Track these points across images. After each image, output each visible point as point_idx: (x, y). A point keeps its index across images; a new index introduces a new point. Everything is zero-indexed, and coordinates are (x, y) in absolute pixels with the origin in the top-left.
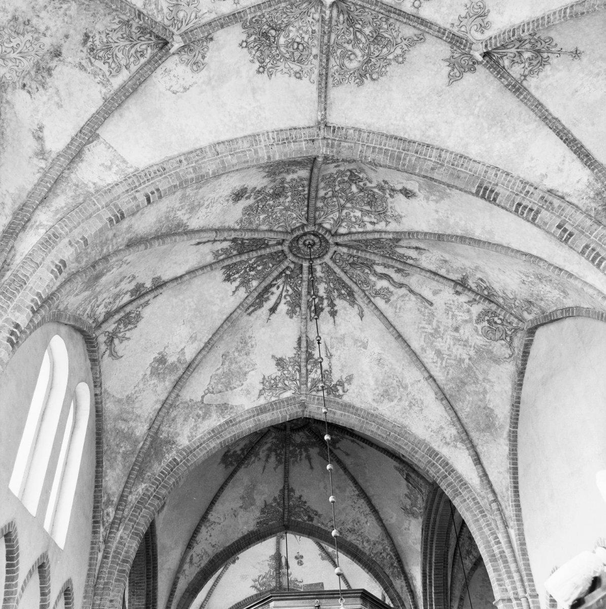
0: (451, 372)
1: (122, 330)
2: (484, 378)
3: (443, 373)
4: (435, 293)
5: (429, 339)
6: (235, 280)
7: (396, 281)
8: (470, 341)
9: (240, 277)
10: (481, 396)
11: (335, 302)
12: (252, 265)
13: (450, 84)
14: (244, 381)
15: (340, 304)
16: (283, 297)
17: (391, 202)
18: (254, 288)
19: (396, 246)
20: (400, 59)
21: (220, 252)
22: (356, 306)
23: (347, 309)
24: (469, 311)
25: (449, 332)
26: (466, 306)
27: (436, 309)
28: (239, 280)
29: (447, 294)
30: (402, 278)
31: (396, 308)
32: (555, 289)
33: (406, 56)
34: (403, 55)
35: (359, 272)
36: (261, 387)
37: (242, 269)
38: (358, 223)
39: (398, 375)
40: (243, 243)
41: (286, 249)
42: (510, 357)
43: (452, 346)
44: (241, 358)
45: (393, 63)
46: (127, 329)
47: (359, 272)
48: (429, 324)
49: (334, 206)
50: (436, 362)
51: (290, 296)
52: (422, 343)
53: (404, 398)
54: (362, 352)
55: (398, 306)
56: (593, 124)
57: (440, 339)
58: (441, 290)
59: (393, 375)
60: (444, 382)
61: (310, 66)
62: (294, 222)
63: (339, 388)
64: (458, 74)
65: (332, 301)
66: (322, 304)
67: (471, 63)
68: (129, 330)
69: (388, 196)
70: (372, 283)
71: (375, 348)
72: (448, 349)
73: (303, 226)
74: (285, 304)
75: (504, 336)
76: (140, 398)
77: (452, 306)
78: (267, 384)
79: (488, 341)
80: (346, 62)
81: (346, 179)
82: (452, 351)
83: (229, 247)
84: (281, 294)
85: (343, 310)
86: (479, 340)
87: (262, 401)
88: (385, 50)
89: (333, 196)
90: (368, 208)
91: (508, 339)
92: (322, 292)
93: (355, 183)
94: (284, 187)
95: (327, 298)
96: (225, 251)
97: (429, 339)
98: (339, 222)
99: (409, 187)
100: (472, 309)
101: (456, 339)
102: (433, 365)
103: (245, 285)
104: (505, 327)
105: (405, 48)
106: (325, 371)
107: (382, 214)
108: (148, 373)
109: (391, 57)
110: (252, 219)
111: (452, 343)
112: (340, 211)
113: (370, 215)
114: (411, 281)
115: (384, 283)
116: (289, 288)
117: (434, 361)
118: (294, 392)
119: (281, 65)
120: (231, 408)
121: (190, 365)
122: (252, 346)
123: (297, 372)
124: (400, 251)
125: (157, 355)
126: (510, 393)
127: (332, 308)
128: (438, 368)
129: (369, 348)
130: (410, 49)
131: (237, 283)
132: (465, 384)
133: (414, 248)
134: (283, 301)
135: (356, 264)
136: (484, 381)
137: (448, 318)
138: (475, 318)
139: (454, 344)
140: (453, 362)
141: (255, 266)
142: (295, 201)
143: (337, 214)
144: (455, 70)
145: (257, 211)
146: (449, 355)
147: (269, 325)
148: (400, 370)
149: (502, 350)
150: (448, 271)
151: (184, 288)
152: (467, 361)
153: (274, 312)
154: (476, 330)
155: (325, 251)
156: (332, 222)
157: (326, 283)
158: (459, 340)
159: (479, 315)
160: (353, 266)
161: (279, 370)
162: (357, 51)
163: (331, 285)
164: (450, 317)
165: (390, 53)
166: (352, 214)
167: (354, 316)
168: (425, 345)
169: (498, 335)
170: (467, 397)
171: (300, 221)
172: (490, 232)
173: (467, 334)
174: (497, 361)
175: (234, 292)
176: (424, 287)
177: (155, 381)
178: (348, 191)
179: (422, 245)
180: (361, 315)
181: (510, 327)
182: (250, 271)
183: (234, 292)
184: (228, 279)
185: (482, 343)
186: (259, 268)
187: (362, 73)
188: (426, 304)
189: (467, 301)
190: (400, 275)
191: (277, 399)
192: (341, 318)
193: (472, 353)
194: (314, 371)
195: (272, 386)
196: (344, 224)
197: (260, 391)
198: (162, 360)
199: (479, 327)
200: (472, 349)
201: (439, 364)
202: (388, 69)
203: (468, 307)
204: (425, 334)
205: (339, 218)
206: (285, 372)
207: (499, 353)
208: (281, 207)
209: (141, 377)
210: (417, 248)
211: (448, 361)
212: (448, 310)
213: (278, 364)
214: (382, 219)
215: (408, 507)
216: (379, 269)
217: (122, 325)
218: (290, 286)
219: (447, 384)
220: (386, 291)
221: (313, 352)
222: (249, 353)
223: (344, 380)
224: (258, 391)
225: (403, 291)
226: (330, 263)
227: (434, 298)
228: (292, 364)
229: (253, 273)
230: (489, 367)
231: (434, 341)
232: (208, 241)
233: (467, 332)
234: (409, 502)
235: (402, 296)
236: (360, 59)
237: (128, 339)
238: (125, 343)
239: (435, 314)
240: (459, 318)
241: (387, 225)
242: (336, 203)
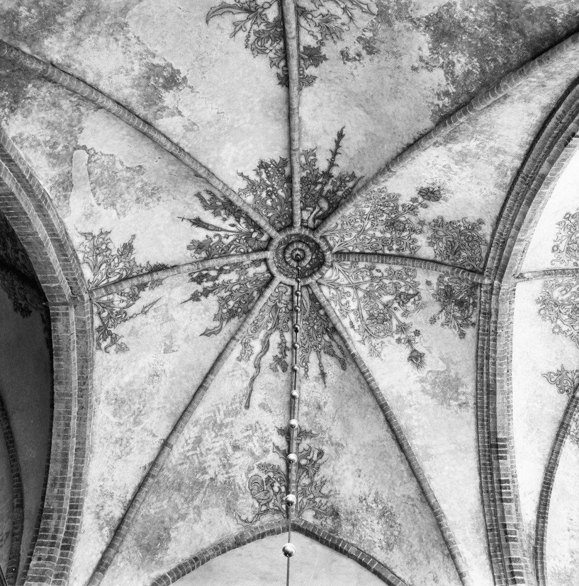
0: (185, 466)
1: (255, 27)
2: (198, 507)
3: (180, 459)
4: (263, 406)
5: (210, 423)
6: (259, 174)
7: (262, 359)
8: (233, 469)
9: (261, 180)
10: (176, 516)
11: (211, 295)
12: (275, 194)
13: (543, 375)
14: (104, 205)
15: (212, 303)
16: (218, 232)
17: (389, 342)
18: (244, 199)
19: (318, 353)
20: (557, 330)
21: (312, 158)
22: (217, 324)
23: (207, 313)
24: (266, 451)
25: (227, 441)
26: (269, 446)
27: (245, 414)
28: (258, 179)
29: (274, 421)
30: (268, 365)
31: (233, 371)
32: (384, 535)
33: (560, 335)
34: (560, 331)
35: (267, 317)
36: (96, 233)
37: (271, 182)
38: (343, 308)
39: (148, 405)
40: (316, 184)
41: (296, 230)
42: (245, 521)
43: (212, 452)
44: (133, 192)
45: (553, 325)
46: (252, 34)
47: (267, 317)
48: (225, 415)
49: (357, 278)
50: (188, 444)
51: (220, 240)
52: (203, 418)
53: (123, 428)
54: (160, 349)
55: (235, 373)
56: (558, 500)
57: (213, 434)
58: (271, 412)
59: (144, 401)
60: (170, 465)
61: (566, 259)
62: (337, 239)
63: (109, 340)
64: (553, 380)
65: (211, 291)
66: (207, 281)
67: (566, 388)
68: (248, 36)
69: (396, 336)
70: (256, 336)
71: (170, 363)
72: (208, 449)
73: (330, 249)
74: (207, 236)
75: (264, 502)
76: (113, 46)
77: (259, 431)
78: (101, 240)
79: (247, 488)
80: (561, 288)
81: (403, 290)
82: (207, 454)
83: (316, 168)
84: (222, 230)
85: (202, 307)
86: (241, 479)
87: (77, 240)
88: (566, 317)
89: (373, 278)
90: (366, 316)
91: (264, 508)
92: (223, 278)
93: (395, 299)
94: (404, 230)
95: (215, 285)
96: (310, 164)
97: (210, 423)
98: (334, 285)
99: (428, 359)
100: (271, 453)
101: (224, 453)
102: (183, 442)
103: (250, 187)
104: (274, 498)
105: (570, 333)
106: (125, 313)
107: (368, 334)
108: (156, 61)
109: (559, 322)
110: (371, 201)
111: (217, 450)
112: (349, 285)
113: (359, 319)
114: (266, 376)
115: (257, 346)
116: (231, 238)
117: (189, 441)
118: (91, 281)
119: (565, 233)
120: (65, 196)
121: (149, 124)
122: (146, 205)
123: (118, 276)
124: (313, 357)
125: (182, 76)
126: (205, 547)
127: (202, 294)
128: (182, 450)
129: (167, 355)
130: (568, 337)
131: (253, 177)
132: (179, 490)
133: (322, 371)
134: (211, 234)
135: (276, 312)
136: (194, 508)
137: (242, 432)
138: (263, 461)
139: (217, 453)
140: (197, 463)
141: (274, 197)
142: (374, 240)
143: (346, 282)
144: (556, 377)
145: (381, 205)
146: (201, 454)
147: (173, 220)
148: (156, 406)
149: (247, 508)
150: (307, 414)
151: (270, 113)
152: (207, 477)
153: (194, 224)
154: (250, 470)
155: (286, 273)
156: (334, 278)
157: (238, 280)
158: (226, 457)
159: (270, 465)
160: (274, 309)
161: (118, 250)
162: (568, 295)
163: (237, 287)
164: (245, 434)
165: (563, 321)
166: (350, 299)
167: (201, 325)
168: (201, 422)
169: (261, 495)
170: (165, 502)
171: (337, 245)
172: (429, 456)
173: (240, 462)
174: (230, 509)
175: (242, 175)
176: (263, 392)
177: (138, 69)
178: (382, 292)
179: (331, 379)
180: (207, 333)
181: (278, 504)
182: (268, 192)
183: (242, 175)
184: (263, 165)
185: (240, 483)
186: (269, 202)
187: (547, 302)
188: (245, 401)
189: (276, 445)
190: (271, 361)
191: (81, 260)
192: (192, 309)
193: (221, 478)
194: (123, 298)
195: (98, 249)
196: (333, 291)
197: (91, 234)
198: (173, 81)
199: (256, 471)
200: (226, 476)
201: (186, 448)
202: (548, 321)
203: (271, 449)
204: (213, 415)
205: (340, 285)
206: (116, 260)
207: (240, 507)
208: (369, 226)
209: (152, 49)
210: (323, 375)
211: (195, 457)
212: (252, 428)
213: (125, 246)
214: (362, 334)
216: (275, 338)
217: (264, 28)
218: (235, 240)
219: (169, 470)
220: (249, 353)
221: (147, 289)
222: (138, 203)
223: (119, 342)
224: (90, 231)
225: (252, 371)
226: (275, 283)
227: (257, 408)
228: (128, 265)
229: (264, 195)
230: (217, 505)
231: (208, 428)
232: (338, 145)
233: (241, 460)
235: (246, 372)
236: (560, 298)
237: (234, 34)
238: (231, 29)
239: (239, 416)
240: (250, 444)
241: (359, 342)
242: (361, 280)
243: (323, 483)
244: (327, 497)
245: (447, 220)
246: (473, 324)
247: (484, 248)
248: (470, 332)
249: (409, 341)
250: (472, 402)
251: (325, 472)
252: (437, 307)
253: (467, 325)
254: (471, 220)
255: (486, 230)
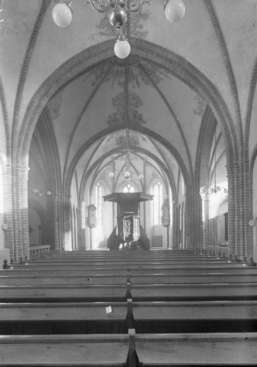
245: (138, 139)
246: (119, 146)
247: (134, 145)
248: (117, 146)
249: (111, 137)
250: (105, 153)
252: (119, 137)
253: (118, 145)
254: (140, 143)
255: (138, 146)
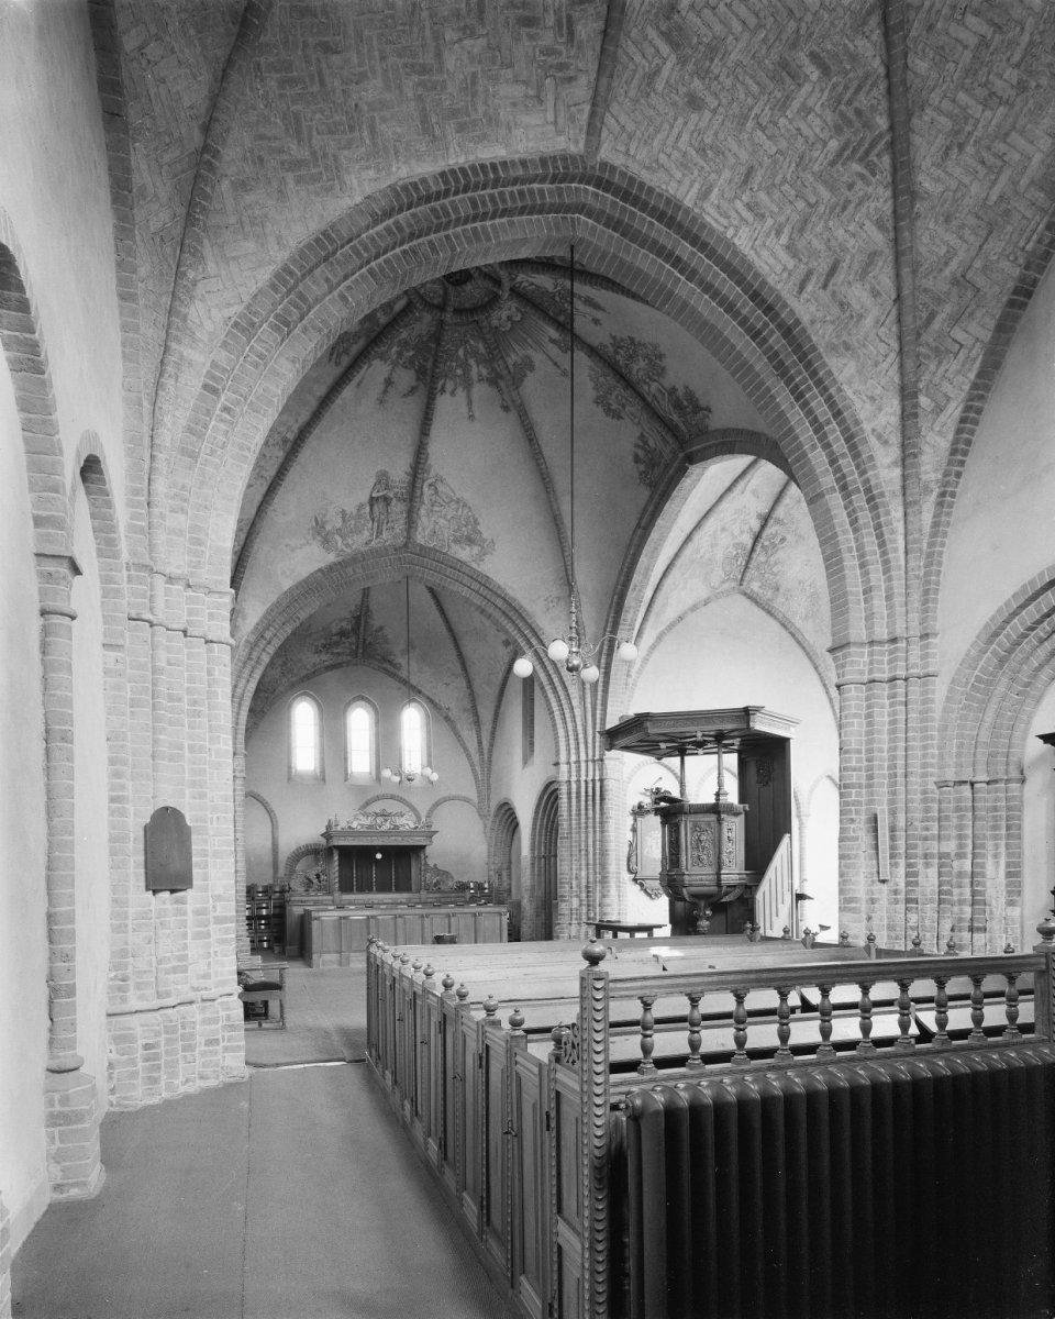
4: (754, 492)
24: (742, 532)
26: (746, 528)
86: (719, 556)
215: (328, 527)
233: (725, 540)
234: (339, 523)
243: (776, 564)
244: (775, 575)
251: (781, 555)
